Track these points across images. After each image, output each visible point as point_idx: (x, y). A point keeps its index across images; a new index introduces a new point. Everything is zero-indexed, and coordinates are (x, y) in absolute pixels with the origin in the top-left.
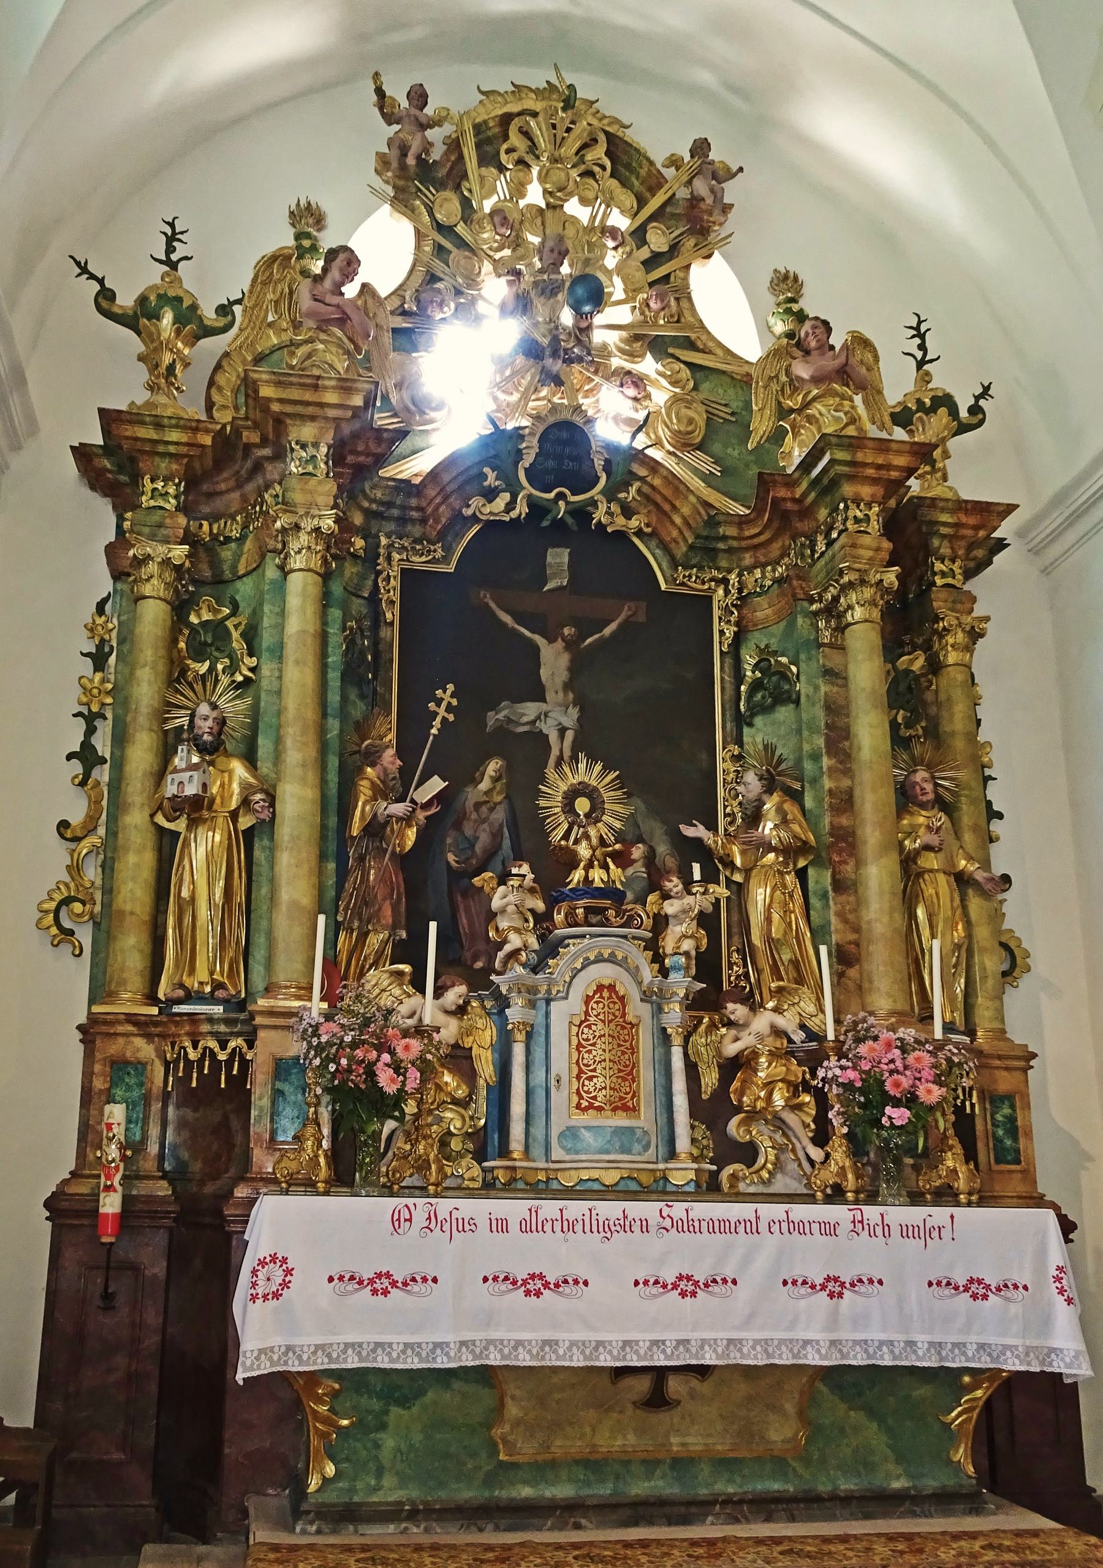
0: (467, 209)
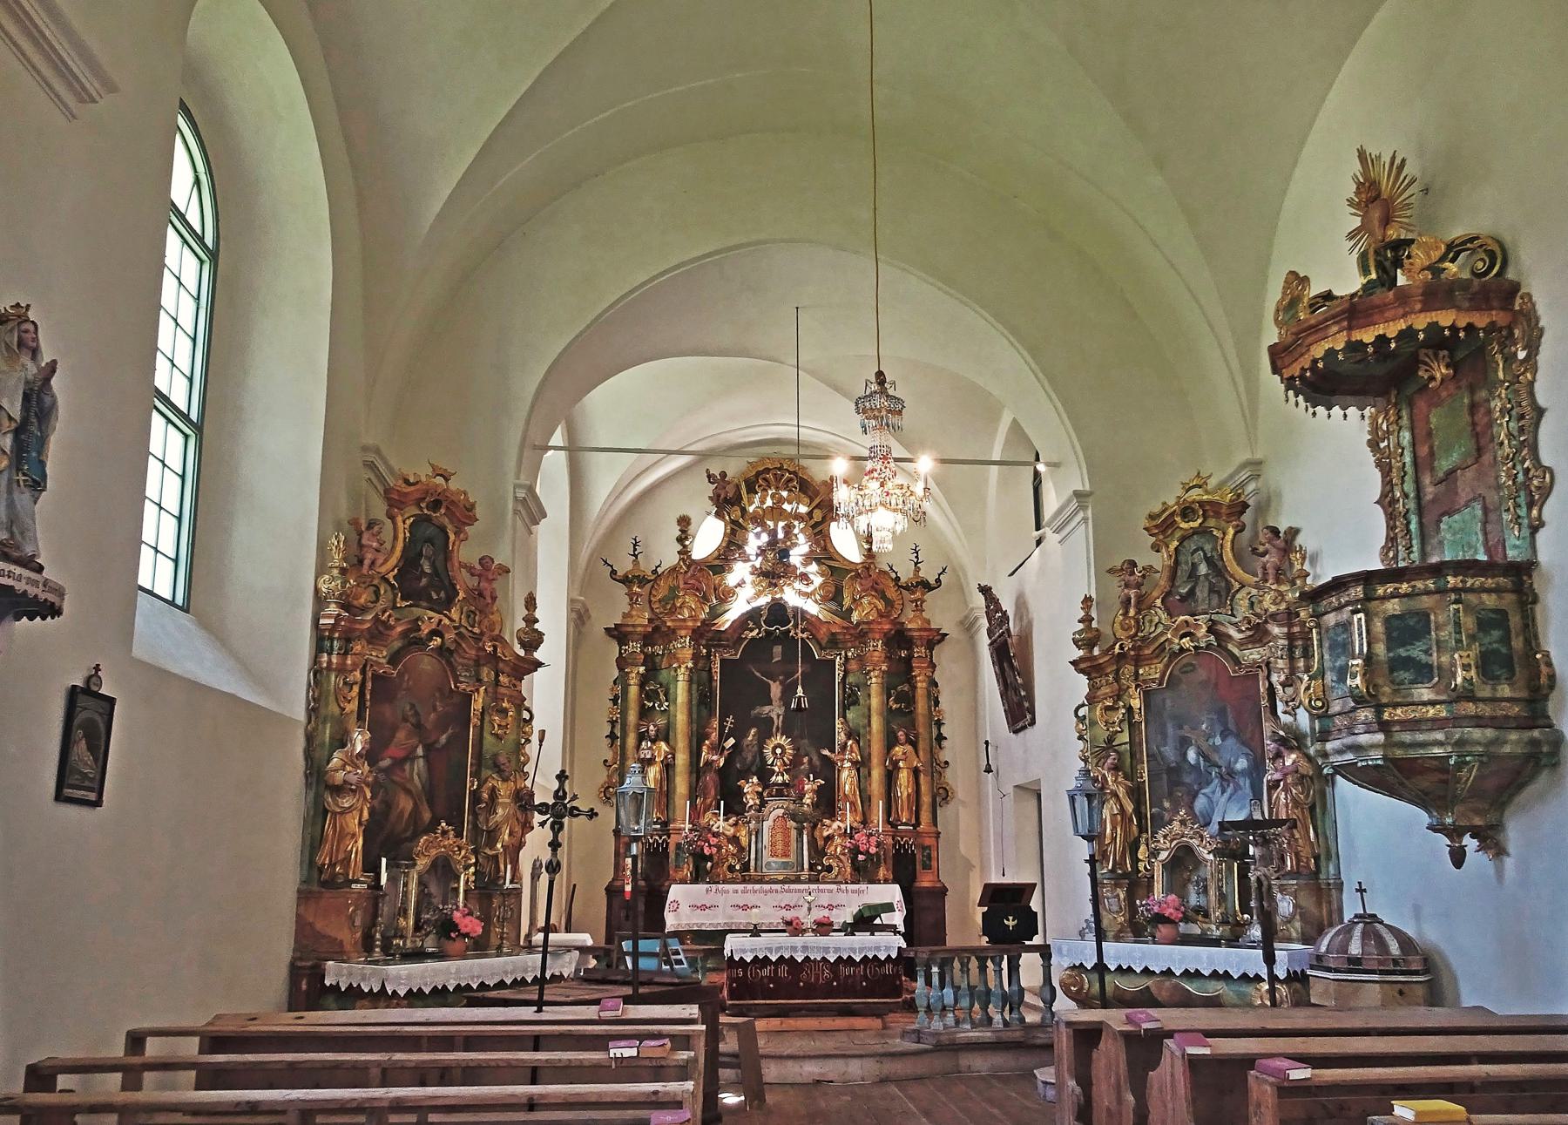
0: (744, 510)
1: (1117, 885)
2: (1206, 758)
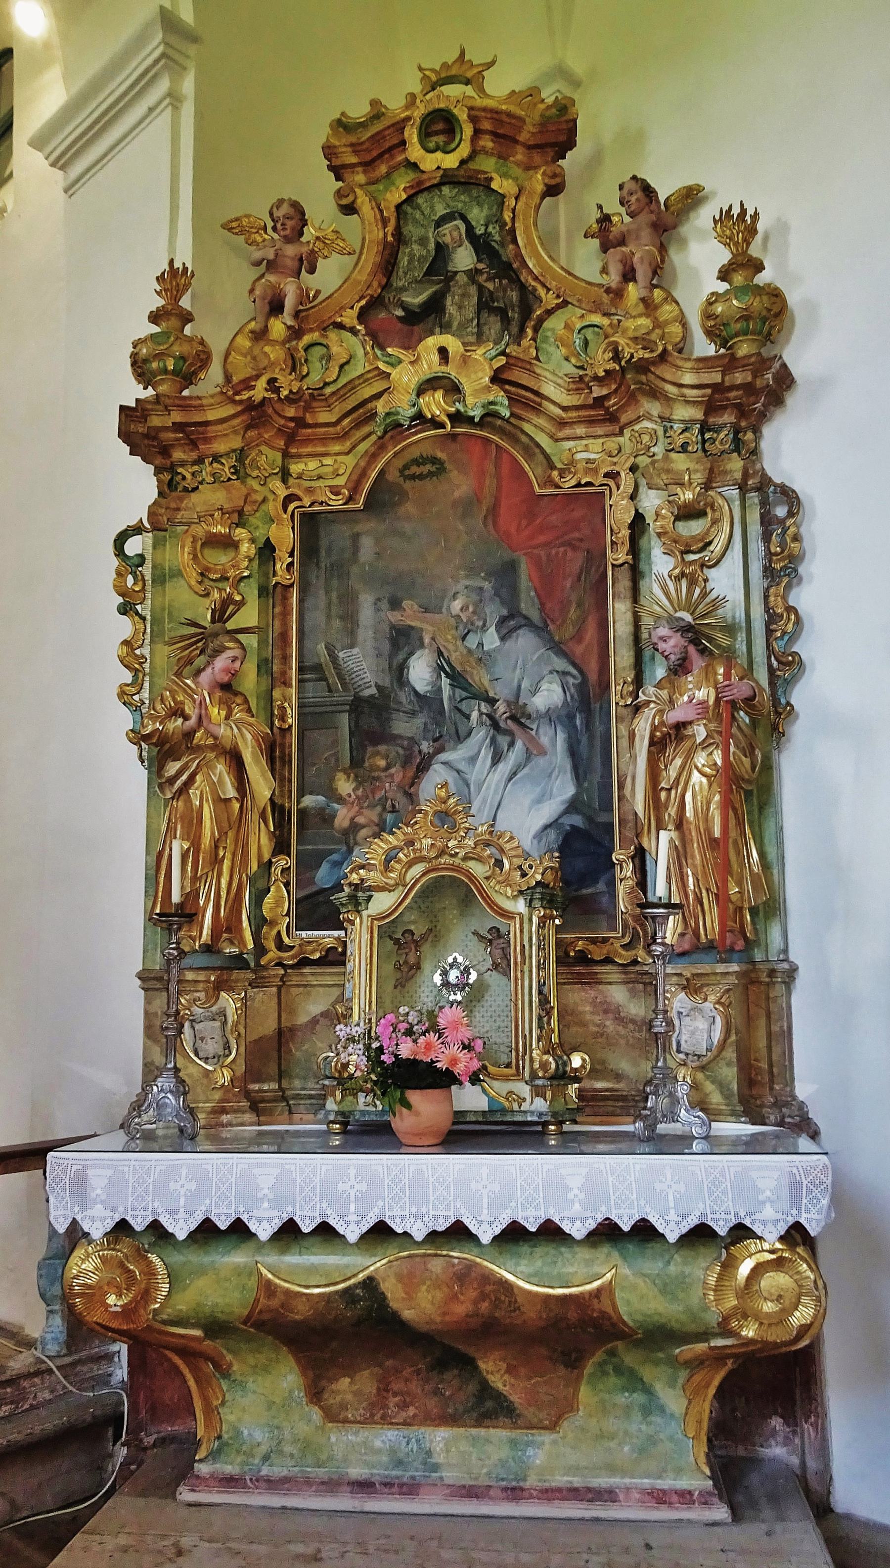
1: (219, 986)
2: (457, 679)
